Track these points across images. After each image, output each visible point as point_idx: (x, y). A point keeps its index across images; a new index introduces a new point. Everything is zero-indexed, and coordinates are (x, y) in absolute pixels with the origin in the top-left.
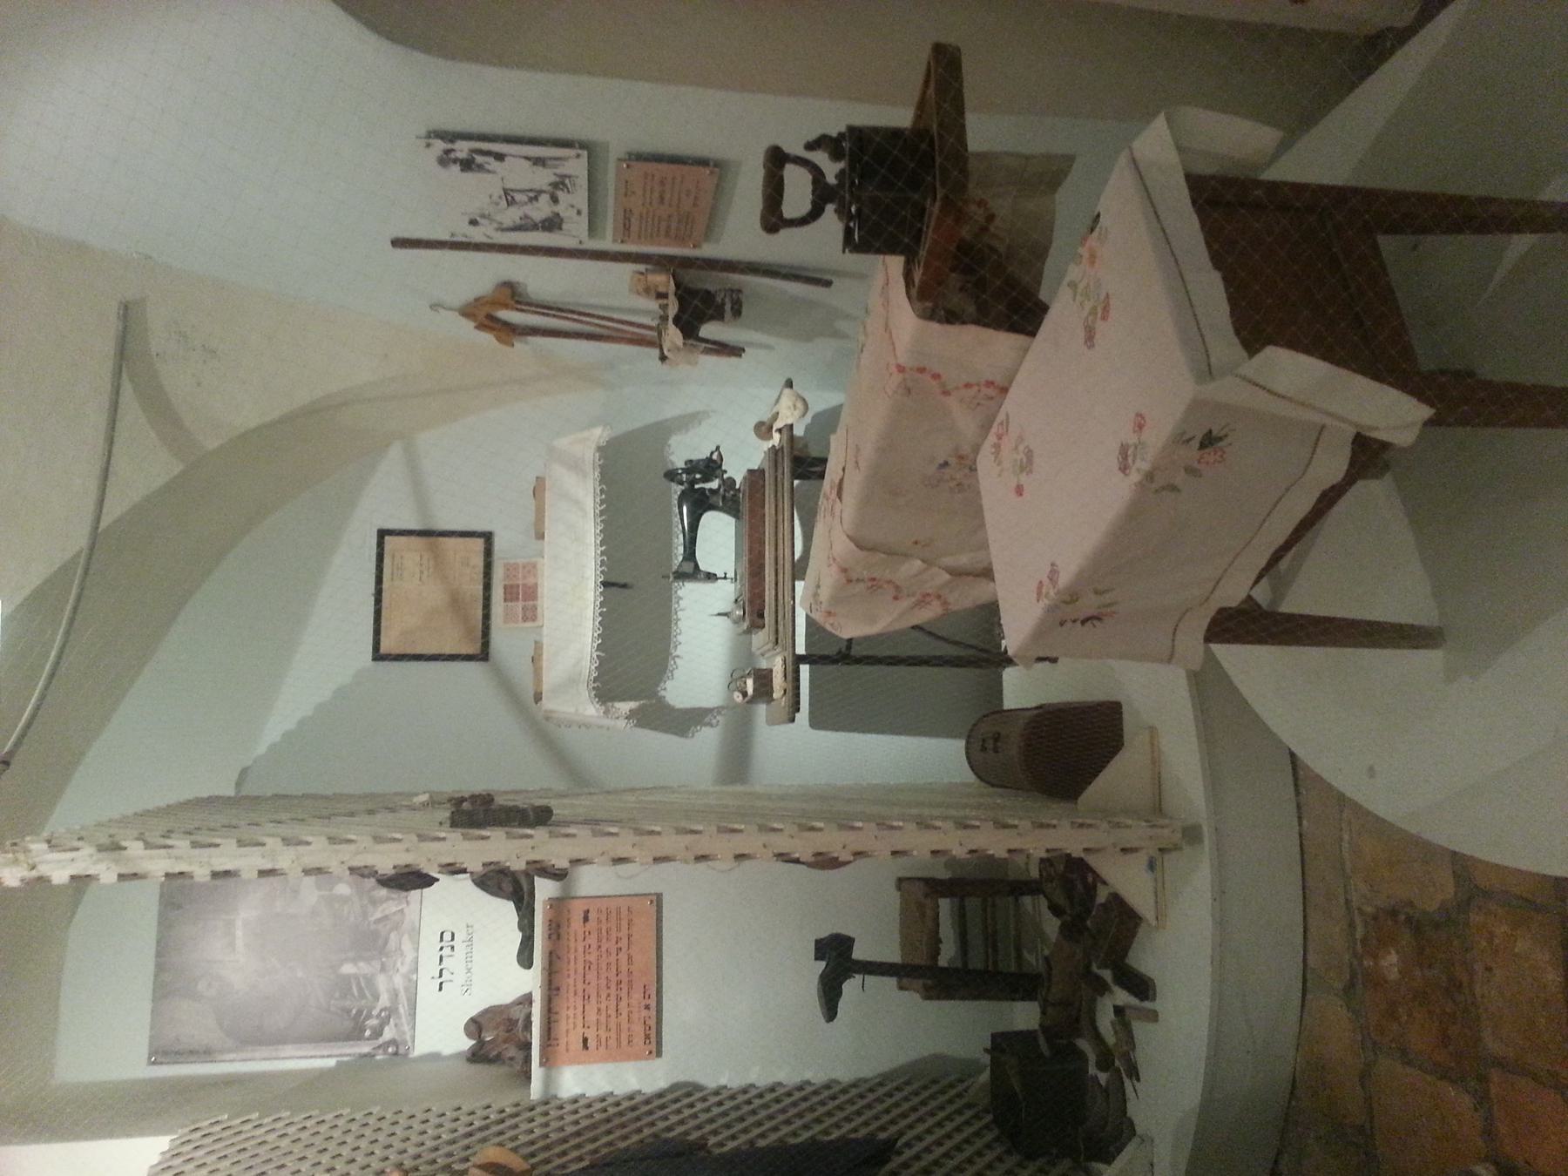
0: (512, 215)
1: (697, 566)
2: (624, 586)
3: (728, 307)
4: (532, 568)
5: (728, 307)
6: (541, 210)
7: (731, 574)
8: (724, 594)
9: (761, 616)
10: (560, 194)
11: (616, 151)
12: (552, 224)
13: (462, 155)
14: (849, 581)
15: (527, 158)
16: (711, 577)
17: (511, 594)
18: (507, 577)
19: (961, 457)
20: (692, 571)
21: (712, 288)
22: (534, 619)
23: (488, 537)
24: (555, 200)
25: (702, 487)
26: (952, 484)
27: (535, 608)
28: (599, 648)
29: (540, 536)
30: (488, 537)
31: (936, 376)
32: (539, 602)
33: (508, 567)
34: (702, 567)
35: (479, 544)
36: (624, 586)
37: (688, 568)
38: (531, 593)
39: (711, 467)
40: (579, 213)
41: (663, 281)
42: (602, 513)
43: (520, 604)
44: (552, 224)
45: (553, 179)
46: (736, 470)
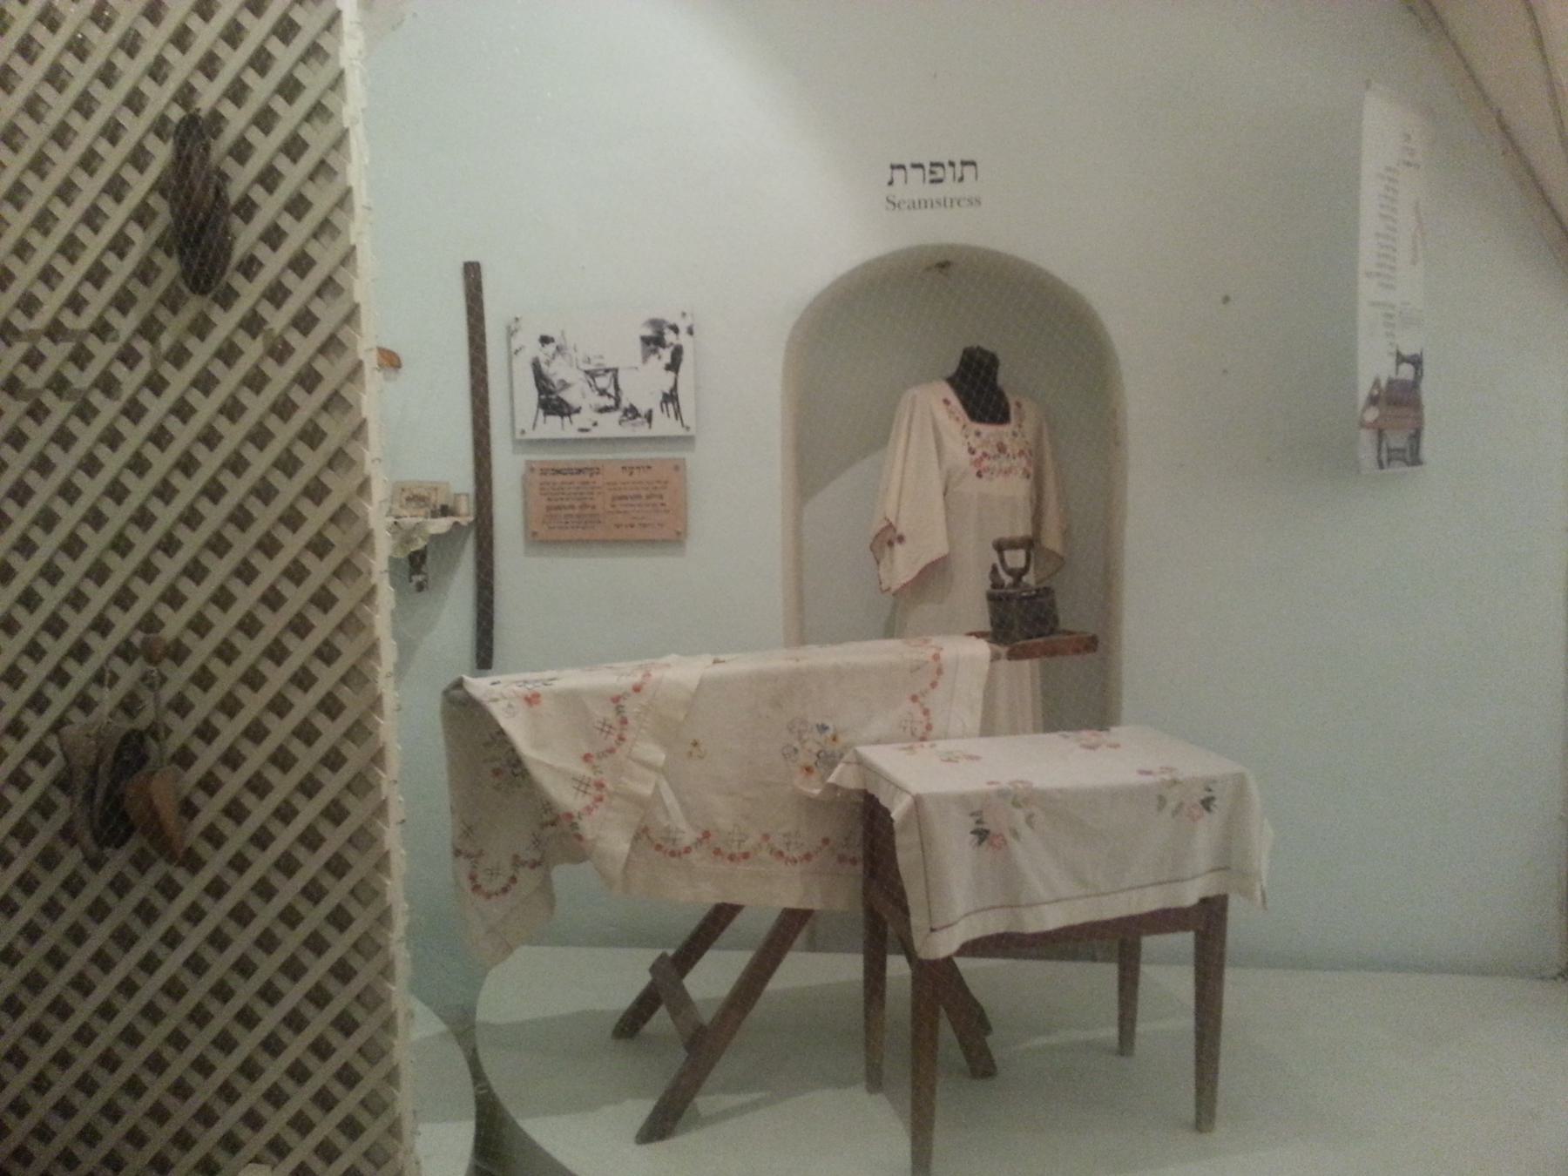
0: (558, 371)
3: (419, 578)
10: (618, 414)
11: (689, 457)
12: (552, 403)
13: (670, 337)
14: (616, 700)
15: (675, 388)
19: (834, 739)
26: (797, 744)
31: (934, 685)
40: (582, 430)
44: (552, 403)
45: (643, 409)
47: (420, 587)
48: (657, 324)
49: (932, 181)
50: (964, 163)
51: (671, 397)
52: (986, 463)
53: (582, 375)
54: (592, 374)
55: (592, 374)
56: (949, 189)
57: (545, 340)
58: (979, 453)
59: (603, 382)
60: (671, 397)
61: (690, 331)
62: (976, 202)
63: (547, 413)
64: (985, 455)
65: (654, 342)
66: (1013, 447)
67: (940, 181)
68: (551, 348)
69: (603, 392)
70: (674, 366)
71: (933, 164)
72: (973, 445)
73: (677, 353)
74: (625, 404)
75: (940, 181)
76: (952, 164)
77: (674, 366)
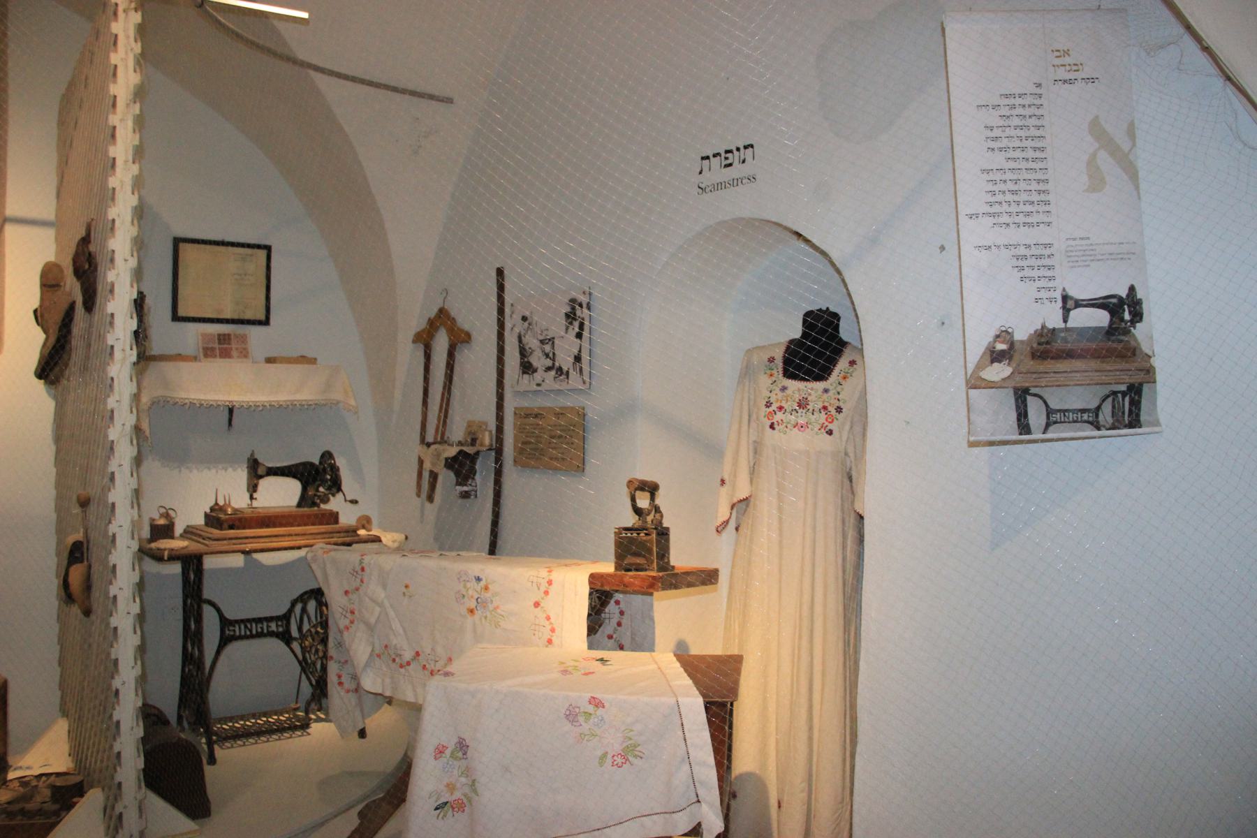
0: (532, 342)
1: (261, 477)
3: (465, 488)
4: (244, 354)
5: (465, 488)
6: (538, 360)
7: (255, 504)
8: (240, 500)
9: (231, 527)
10: (553, 373)
12: (527, 368)
13: (578, 313)
16: (253, 488)
18: (236, 336)
20: (257, 472)
21: (477, 477)
22: (206, 356)
23: (266, 322)
24: (549, 369)
29: (270, 360)
30: (266, 322)
32: (218, 360)
33: (243, 339)
35: (263, 318)
37: (261, 471)
38: (226, 354)
39: (336, 485)
40: (538, 385)
41: (487, 439)
43: (217, 346)
44: (527, 368)
45: (565, 369)
46: (335, 504)
47: (465, 495)
48: (573, 301)
49: (726, 166)
50: (746, 147)
51: (578, 359)
52: (779, 416)
53: (538, 343)
54: (542, 342)
55: (542, 342)
56: (736, 171)
57: (524, 319)
58: (774, 407)
59: (547, 348)
60: (578, 359)
61: (589, 308)
62: (752, 179)
63: (524, 373)
64: (781, 408)
65: (571, 317)
66: (815, 404)
67: (730, 165)
68: (526, 324)
69: (547, 356)
70: (579, 336)
71: (727, 152)
72: (772, 400)
73: (581, 326)
74: (557, 364)
75: (730, 165)
76: (738, 149)
77: (579, 336)
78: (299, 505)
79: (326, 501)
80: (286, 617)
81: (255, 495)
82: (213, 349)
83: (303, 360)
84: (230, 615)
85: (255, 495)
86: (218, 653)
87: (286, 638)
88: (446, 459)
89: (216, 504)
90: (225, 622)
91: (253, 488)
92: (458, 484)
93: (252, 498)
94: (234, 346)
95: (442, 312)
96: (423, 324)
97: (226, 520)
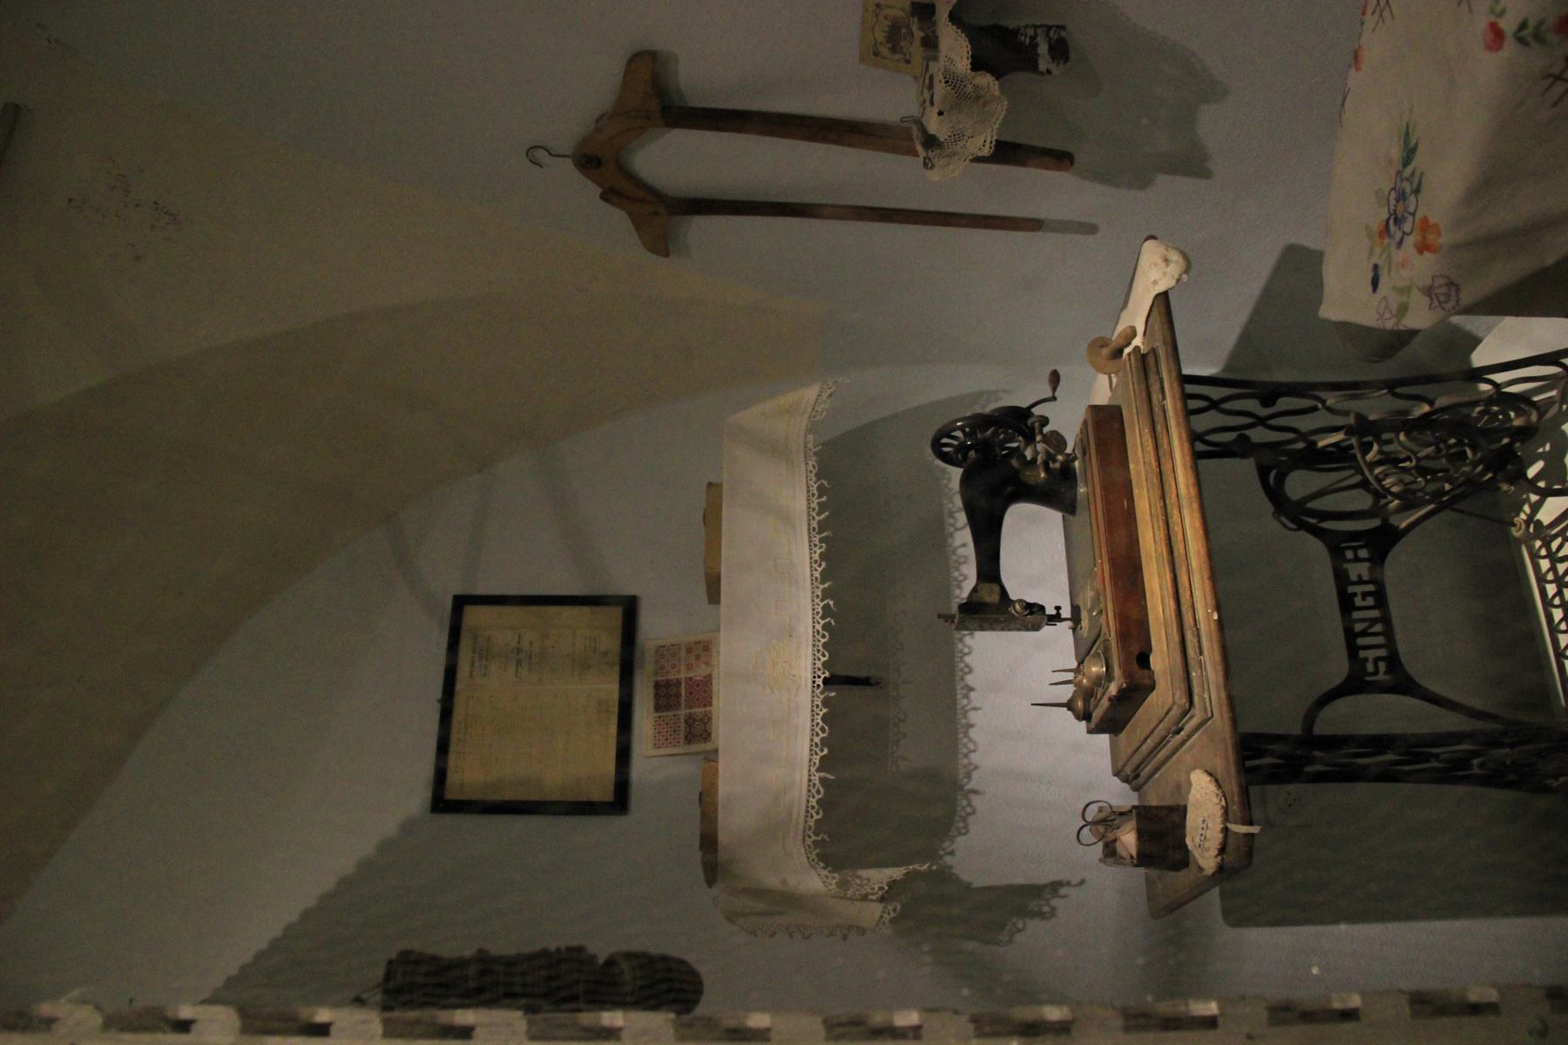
1: (1004, 592)
2: (866, 682)
3: (1043, 49)
4: (703, 649)
5: (1043, 49)
7: (1066, 612)
9: (1143, 660)
16: (1035, 617)
17: (666, 696)
20: (992, 608)
21: (1012, 24)
22: (706, 736)
25: (1000, 461)
27: (707, 719)
28: (824, 765)
30: (630, 608)
32: (714, 709)
33: (663, 652)
34: (1013, 597)
35: (615, 615)
36: (866, 682)
38: (702, 691)
42: (822, 527)
46: (1066, 419)
78: (1068, 507)
79: (1057, 441)
80: (1337, 545)
81: (1050, 611)
82: (690, 721)
83: (712, 518)
84: (1338, 669)
85: (1050, 611)
86: (1436, 700)
87: (1382, 541)
88: (977, 64)
89: (1069, 705)
90: (1355, 684)
91: (1035, 617)
92: (1031, 64)
93: (1056, 618)
94: (682, 676)
95: (588, 161)
96: (617, 219)
97: (1128, 675)
